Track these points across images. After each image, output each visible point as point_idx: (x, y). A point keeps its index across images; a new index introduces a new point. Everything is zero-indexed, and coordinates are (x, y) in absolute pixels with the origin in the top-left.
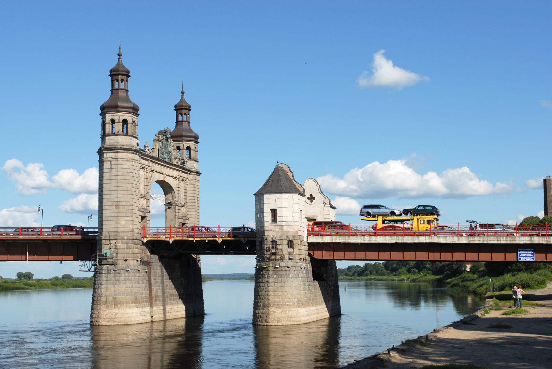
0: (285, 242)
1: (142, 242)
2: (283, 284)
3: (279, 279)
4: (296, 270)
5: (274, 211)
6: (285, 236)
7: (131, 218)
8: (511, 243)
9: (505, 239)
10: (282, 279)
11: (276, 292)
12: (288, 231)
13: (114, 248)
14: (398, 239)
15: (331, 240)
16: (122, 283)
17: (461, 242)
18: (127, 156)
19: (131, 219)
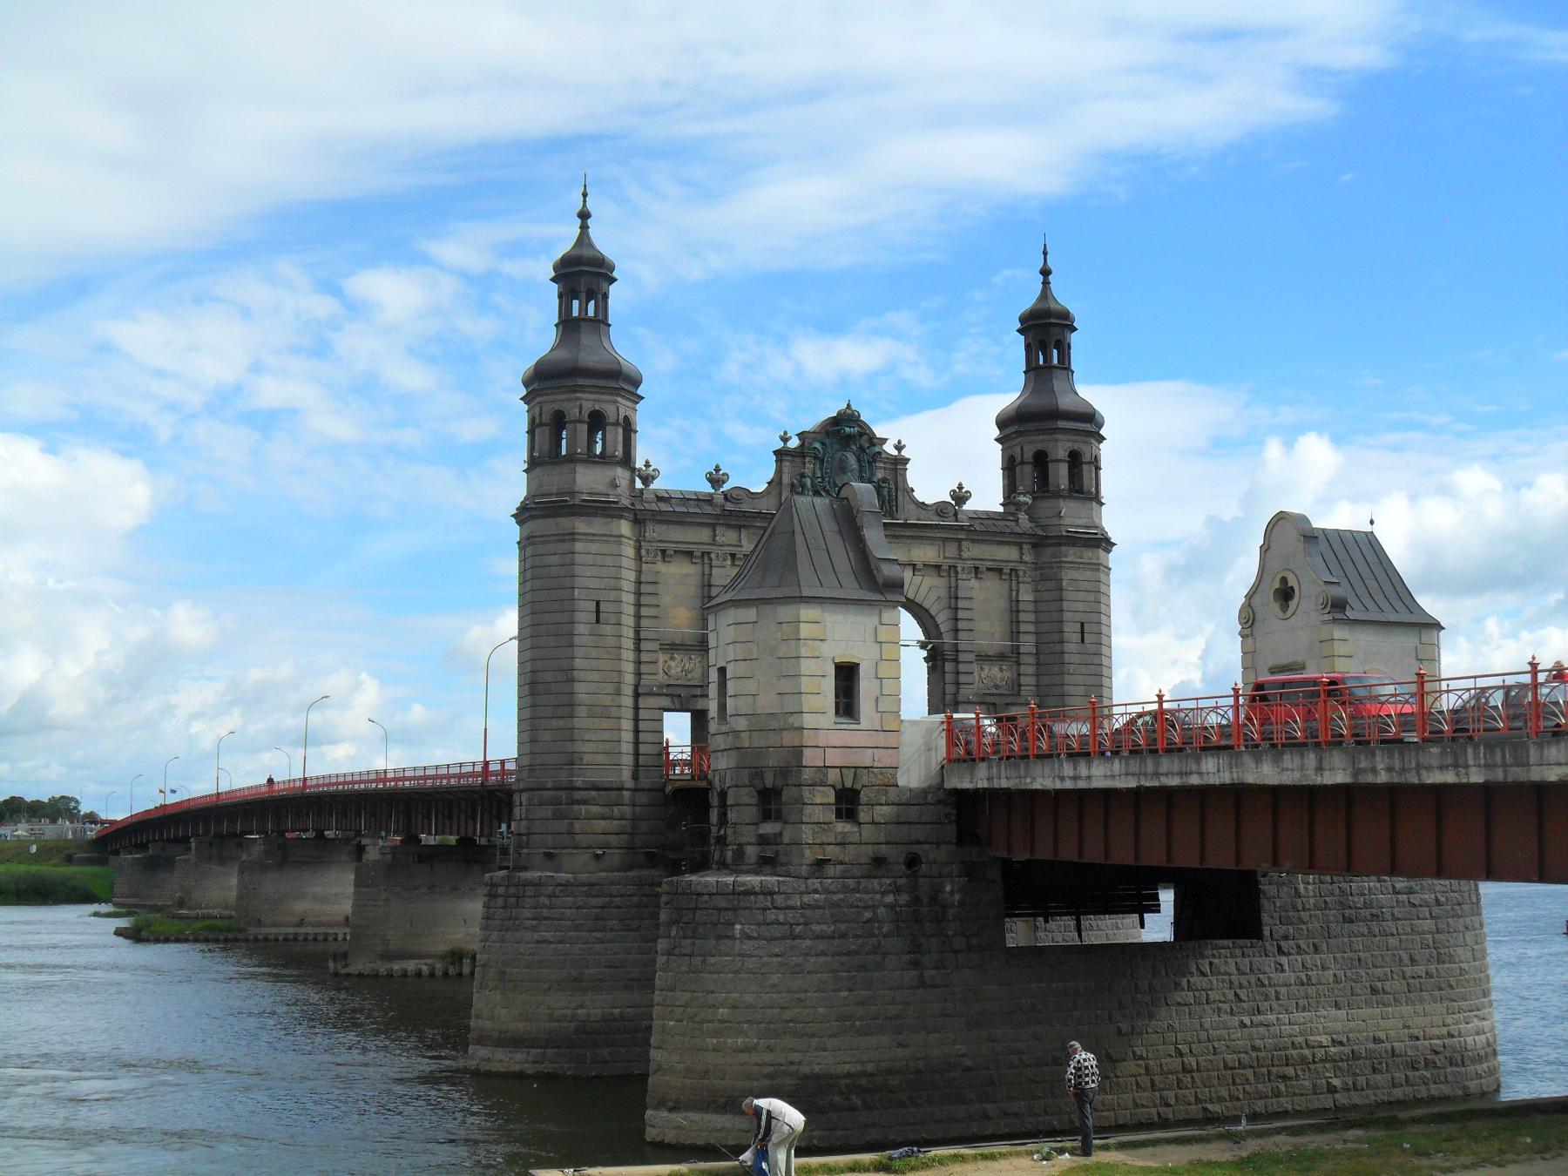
0: (747, 797)
1: (663, 791)
2: (697, 961)
3: (684, 942)
4: (774, 908)
5: (847, 674)
6: (746, 772)
8: (1510, 779)
9: (1485, 758)
10: (698, 942)
16: (525, 928)
17: (1329, 779)
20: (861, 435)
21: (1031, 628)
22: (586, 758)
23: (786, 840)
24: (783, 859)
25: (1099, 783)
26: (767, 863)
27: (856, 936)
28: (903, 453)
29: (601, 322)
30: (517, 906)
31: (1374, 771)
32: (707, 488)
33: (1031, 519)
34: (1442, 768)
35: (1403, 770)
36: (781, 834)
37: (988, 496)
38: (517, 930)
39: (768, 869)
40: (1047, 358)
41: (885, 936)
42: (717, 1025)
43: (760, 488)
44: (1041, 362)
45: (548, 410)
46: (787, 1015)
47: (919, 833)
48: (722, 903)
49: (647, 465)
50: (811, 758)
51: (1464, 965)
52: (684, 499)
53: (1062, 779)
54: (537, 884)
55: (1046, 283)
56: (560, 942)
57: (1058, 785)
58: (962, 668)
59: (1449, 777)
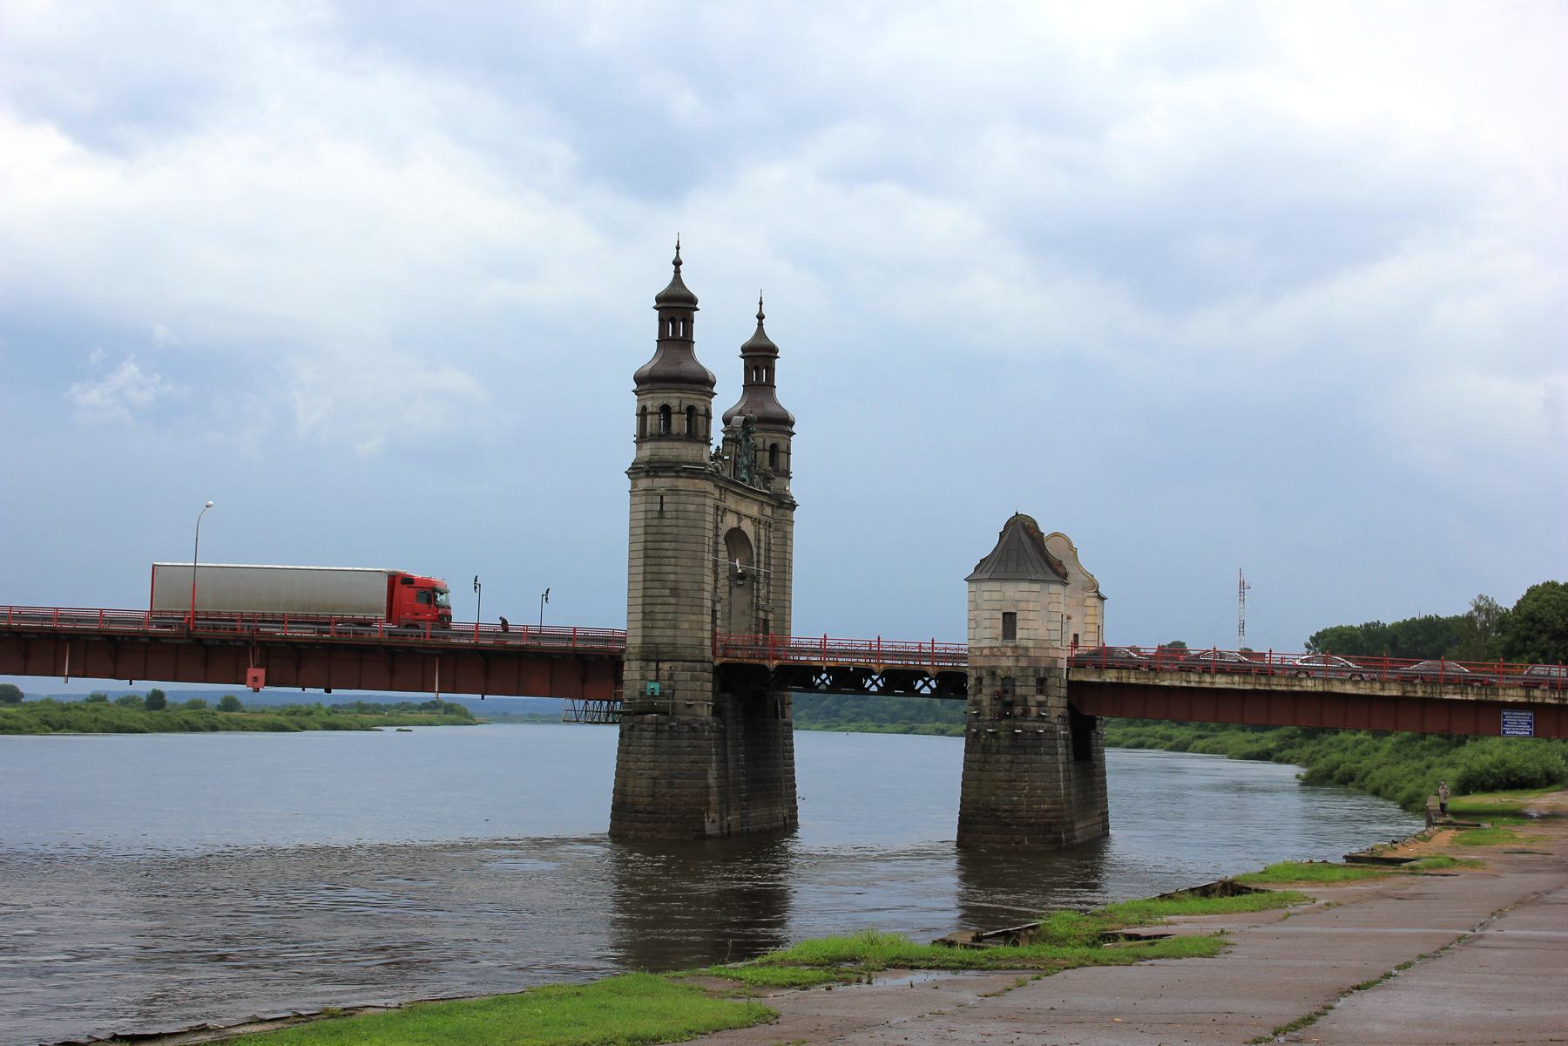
0: (1032, 682)
3: (1020, 756)
7: (700, 616)
8: (1488, 699)
11: (1014, 783)
12: (1037, 659)
13: (666, 677)
14: (1258, 681)
15: (1118, 678)
18: (694, 484)
23: (1049, 705)
29: (687, 342)
31: (1415, 692)
34: (1454, 694)
35: (1432, 693)
36: (1046, 702)
38: (681, 754)
42: (1037, 798)
45: (686, 404)
59: (1458, 697)
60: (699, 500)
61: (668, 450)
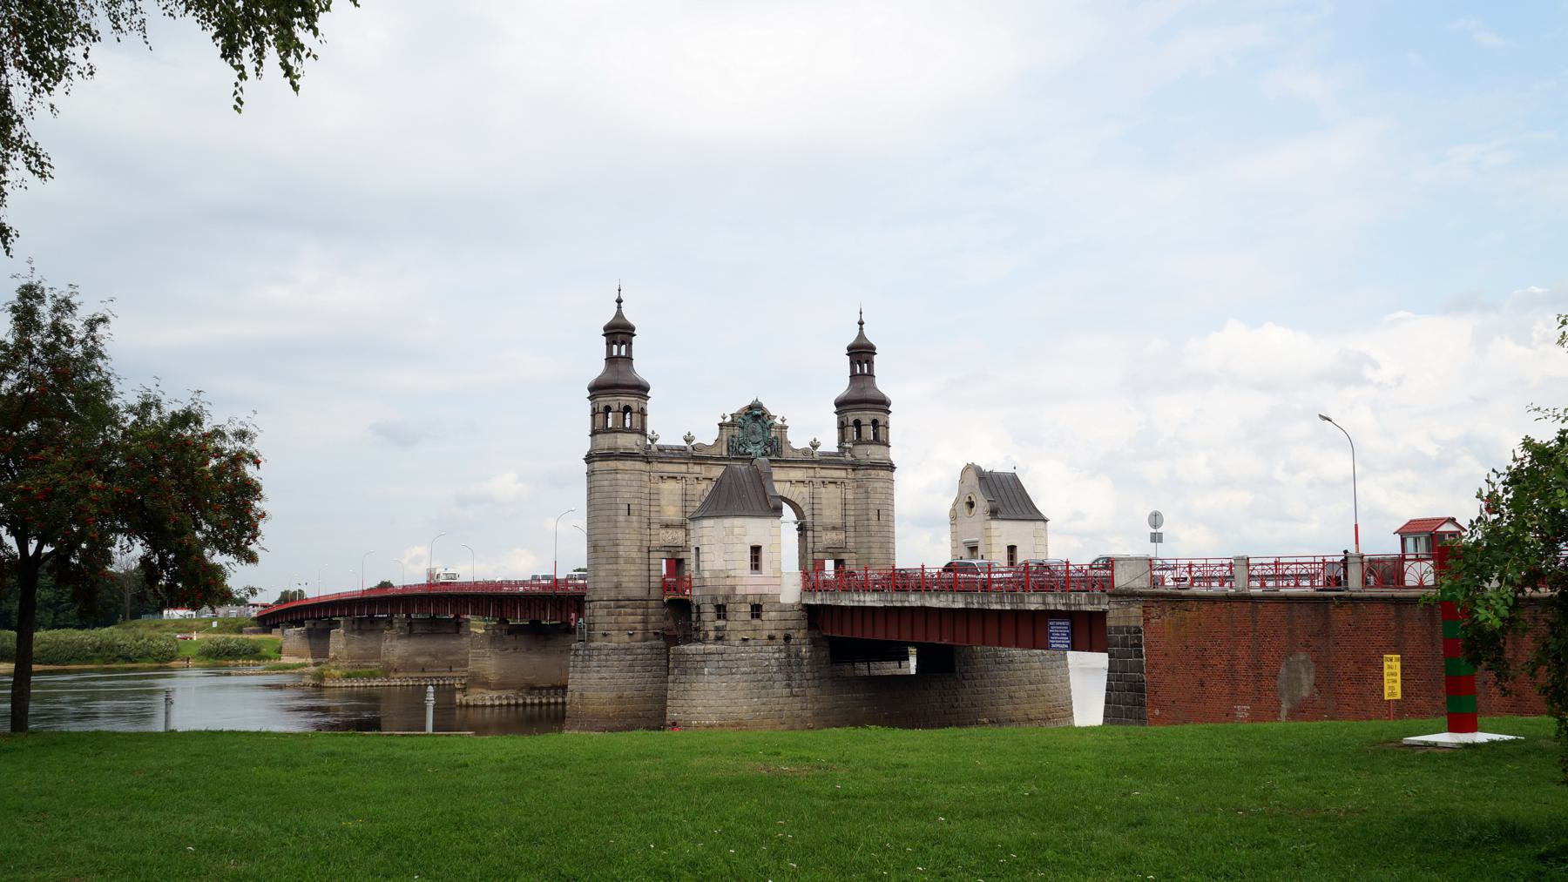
2: (688, 685)
5: (756, 550)
8: (1019, 608)
12: (715, 588)
19: (615, 566)
20: (763, 414)
21: (852, 513)
22: (624, 585)
24: (727, 638)
25: (868, 604)
26: (719, 639)
27: (761, 673)
28: (785, 423)
30: (590, 660)
32: (684, 444)
33: (852, 456)
34: (996, 603)
37: (829, 442)
39: (720, 642)
40: (862, 369)
41: (775, 673)
43: (711, 443)
44: (858, 372)
46: (730, 709)
47: (790, 624)
48: (699, 659)
49: (653, 433)
50: (740, 591)
51: (1056, 685)
52: (672, 449)
53: (853, 601)
54: (599, 649)
55: (861, 329)
56: (611, 678)
57: (852, 604)
58: (816, 534)
60: (613, 476)
61: (605, 441)
